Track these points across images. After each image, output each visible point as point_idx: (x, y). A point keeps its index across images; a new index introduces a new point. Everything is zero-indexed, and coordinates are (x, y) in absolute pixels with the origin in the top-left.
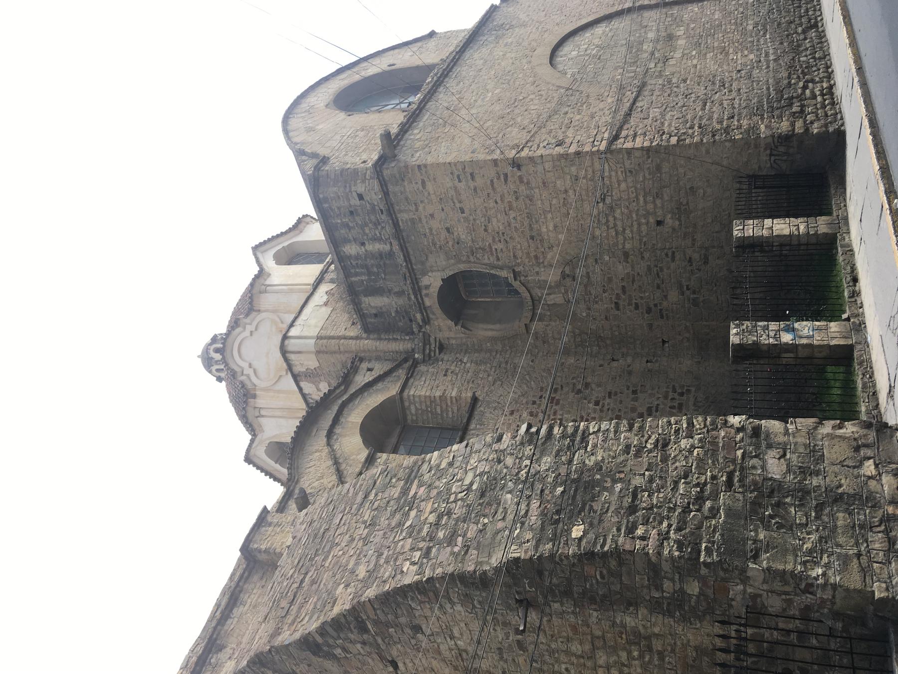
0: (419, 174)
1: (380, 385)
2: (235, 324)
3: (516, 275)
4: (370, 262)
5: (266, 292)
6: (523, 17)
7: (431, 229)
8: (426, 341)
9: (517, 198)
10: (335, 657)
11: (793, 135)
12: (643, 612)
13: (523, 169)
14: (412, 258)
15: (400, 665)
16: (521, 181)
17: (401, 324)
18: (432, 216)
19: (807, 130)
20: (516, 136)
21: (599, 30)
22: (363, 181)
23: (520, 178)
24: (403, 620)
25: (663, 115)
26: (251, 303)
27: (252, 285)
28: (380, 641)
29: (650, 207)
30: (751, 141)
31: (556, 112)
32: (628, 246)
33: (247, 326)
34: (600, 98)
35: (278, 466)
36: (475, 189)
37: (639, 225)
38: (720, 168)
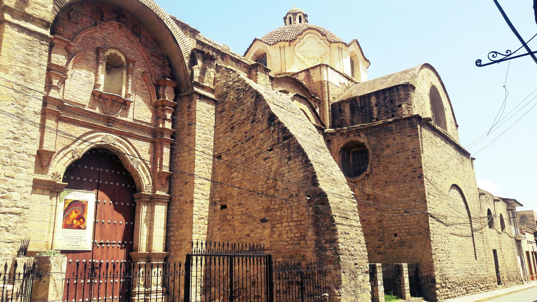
0: (414, 134)
3: (368, 175)
4: (368, 108)
7: (388, 138)
9: (405, 176)
10: (270, 127)
11: (436, 284)
12: (315, 238)
14: (373, 129)
15: (271, 152)
16: (413, 178)
18: (395, 139)
19: (437, 289)
21: (463, 204)
23: (414, 178)
25: (439, 234)
28: (281, 145)
29: (403, 231)
32: (384, 222)
36: (408, 158)
37: (395, 227)
38: (421, 257)
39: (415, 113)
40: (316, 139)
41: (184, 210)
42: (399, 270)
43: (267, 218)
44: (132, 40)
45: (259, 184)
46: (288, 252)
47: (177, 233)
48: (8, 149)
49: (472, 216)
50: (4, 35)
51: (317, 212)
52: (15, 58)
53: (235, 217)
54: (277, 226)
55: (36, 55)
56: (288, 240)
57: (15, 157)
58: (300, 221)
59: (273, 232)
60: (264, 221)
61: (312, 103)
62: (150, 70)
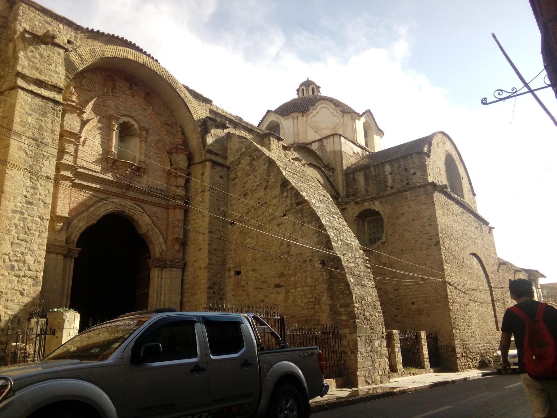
0: (430, 201)
1: (328, 184)
2: (336, 103)
4: (382, 177)
5: (352, 119)
6: (485, 238)
8: (346, 203)
12: (329, 302)
13: (435, 246)
16: (429, 246)
17: (351, 190)
20: (447, 241)
21: (482, 273)
22: (422, 175)
23: (431, 245)
24: (305, 219)
26: (348, 113)
27: (355, 113)
28: (294, 210)
30: (452, 337)
31: (455, 258)
32: (401, 290)
33: (335, 111)
34: (461, 276)
35: (265, 126)
36: (424, 226)
37: (412, 295)
39: (430, 180)
40: (330, 205)
41: (198, 277)
42: (418, 338)
43: (281, 284)
44: (146, 109)
45: (273, 250)
46: (303, 317)
47: (191, 299)
48: (22, 213)
49: (492, 285)
50: (18, 101)
51: (331, 276)
52: (28, 124)
53: (250, 283)
54: (291, 291)
55: (49, 120)
56: (303, 305)
57: (28, 221)
58: (315, 286)
59: (287, 296)
60: (278, 286)
61: (326, 172)
62: (163, 138)
